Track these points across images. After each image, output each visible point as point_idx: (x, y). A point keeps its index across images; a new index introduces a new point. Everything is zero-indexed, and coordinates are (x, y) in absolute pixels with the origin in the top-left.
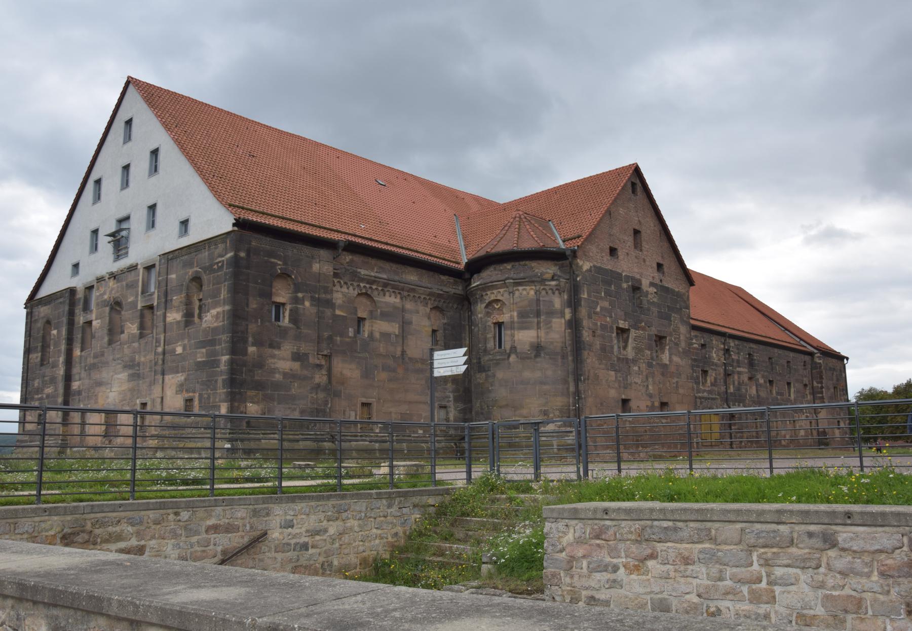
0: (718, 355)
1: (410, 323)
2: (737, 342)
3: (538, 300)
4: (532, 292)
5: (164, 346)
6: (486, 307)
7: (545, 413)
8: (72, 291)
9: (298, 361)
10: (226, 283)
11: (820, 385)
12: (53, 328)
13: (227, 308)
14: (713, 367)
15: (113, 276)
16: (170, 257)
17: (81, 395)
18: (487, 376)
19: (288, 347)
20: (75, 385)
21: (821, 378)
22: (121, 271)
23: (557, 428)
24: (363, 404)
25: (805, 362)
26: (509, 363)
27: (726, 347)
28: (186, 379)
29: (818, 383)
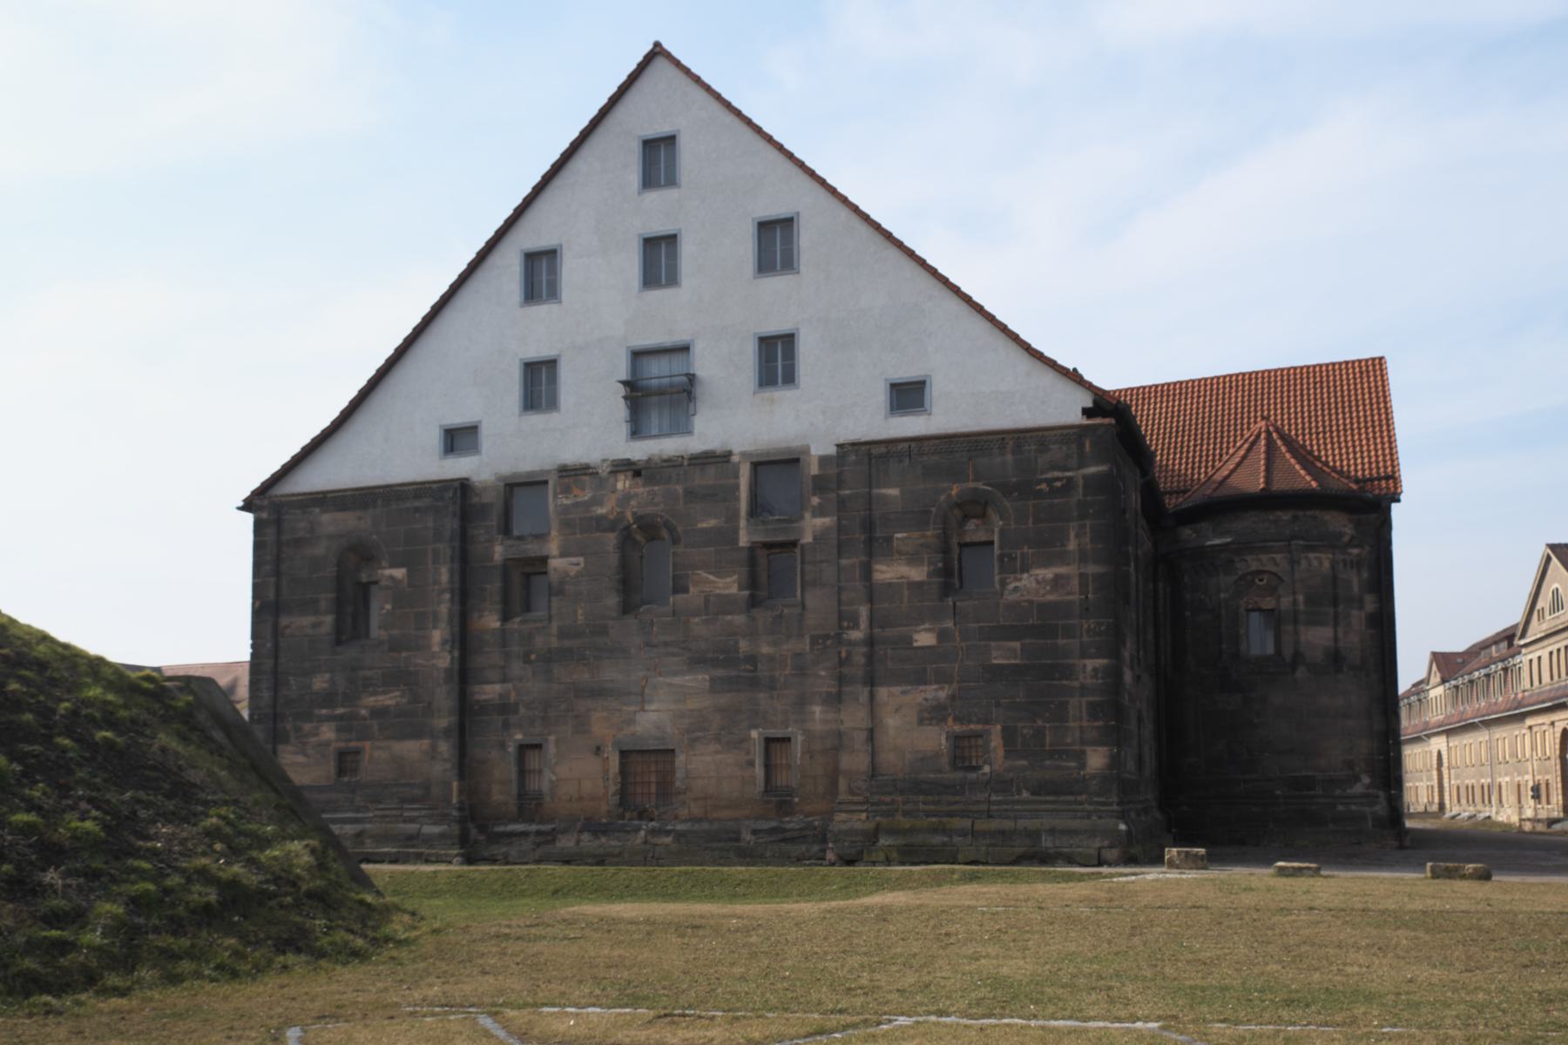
4: (1327, 564)
5: (871, 626)
8: (463, 487)
10: (1088, 523)
12: (384, 563)
13: (1092, 569)
15: (634, 469)
17: (516, 712)
20: (490, 691)
22: (665, 461)
23: (1365, 791)
28: (952, 698)
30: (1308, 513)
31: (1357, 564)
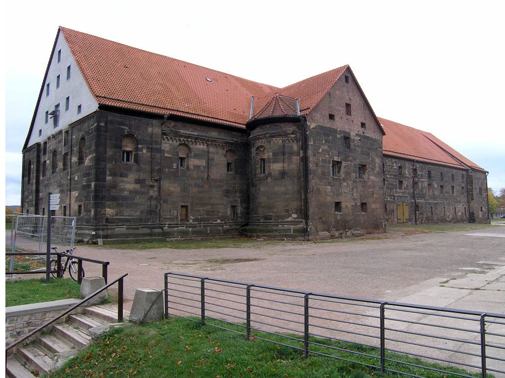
0: (409, 172)
1: (213, 159)
2: (421, 165)
3: (284, 146)
4: (281, 141)
6: (256, 150)
7: (287, 211)
9: (139, 184)
11: (471, 187)
13: (94, 155)
16: (73, 125)
18: (256, 189)
19: (132, 176)
24: (182, 206)
25: (463, 175)
26: (267, 182)
30: (275, 124)
31: (297, 140)
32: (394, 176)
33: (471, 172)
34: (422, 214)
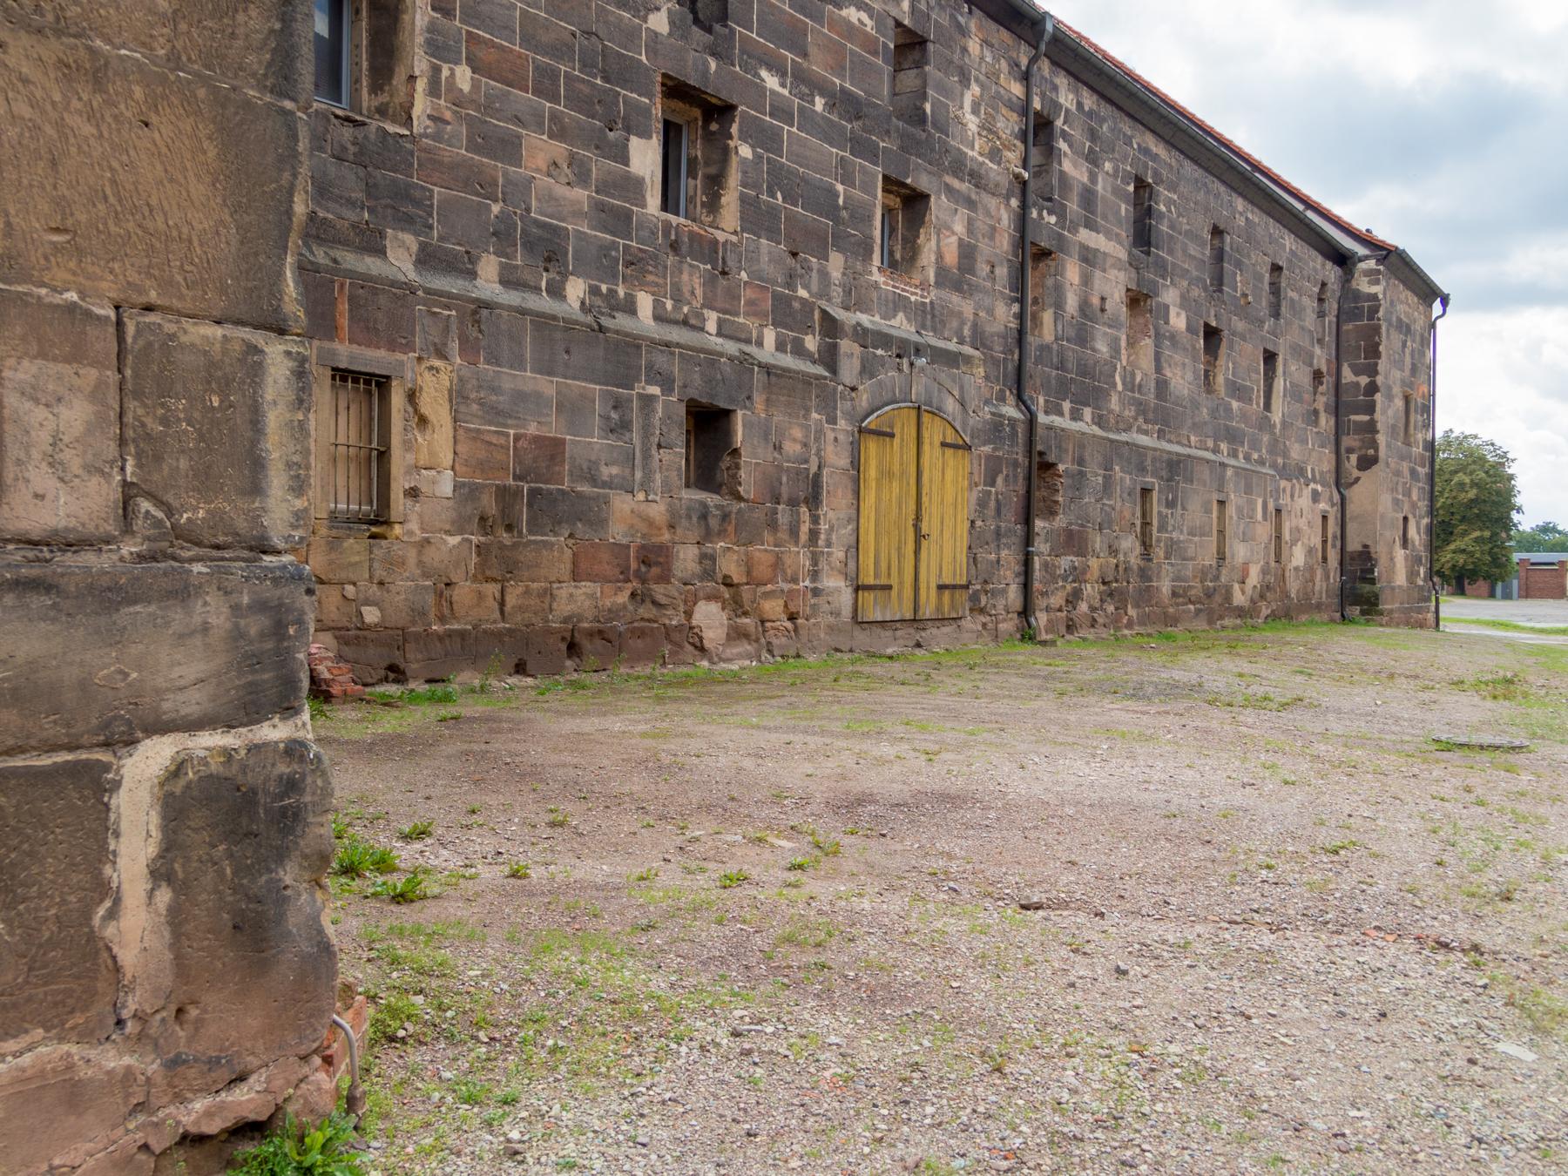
0: (988, 128)
11: (1364, 380)
14: (956, 184)
21: (1374, 352)
27: (1037, 104)
29: (1357, 371)
32: (843, 102)
33: (1373, 276)
34: (1073, 541)
